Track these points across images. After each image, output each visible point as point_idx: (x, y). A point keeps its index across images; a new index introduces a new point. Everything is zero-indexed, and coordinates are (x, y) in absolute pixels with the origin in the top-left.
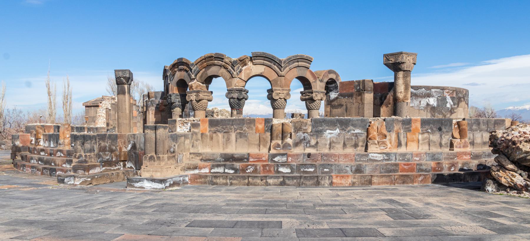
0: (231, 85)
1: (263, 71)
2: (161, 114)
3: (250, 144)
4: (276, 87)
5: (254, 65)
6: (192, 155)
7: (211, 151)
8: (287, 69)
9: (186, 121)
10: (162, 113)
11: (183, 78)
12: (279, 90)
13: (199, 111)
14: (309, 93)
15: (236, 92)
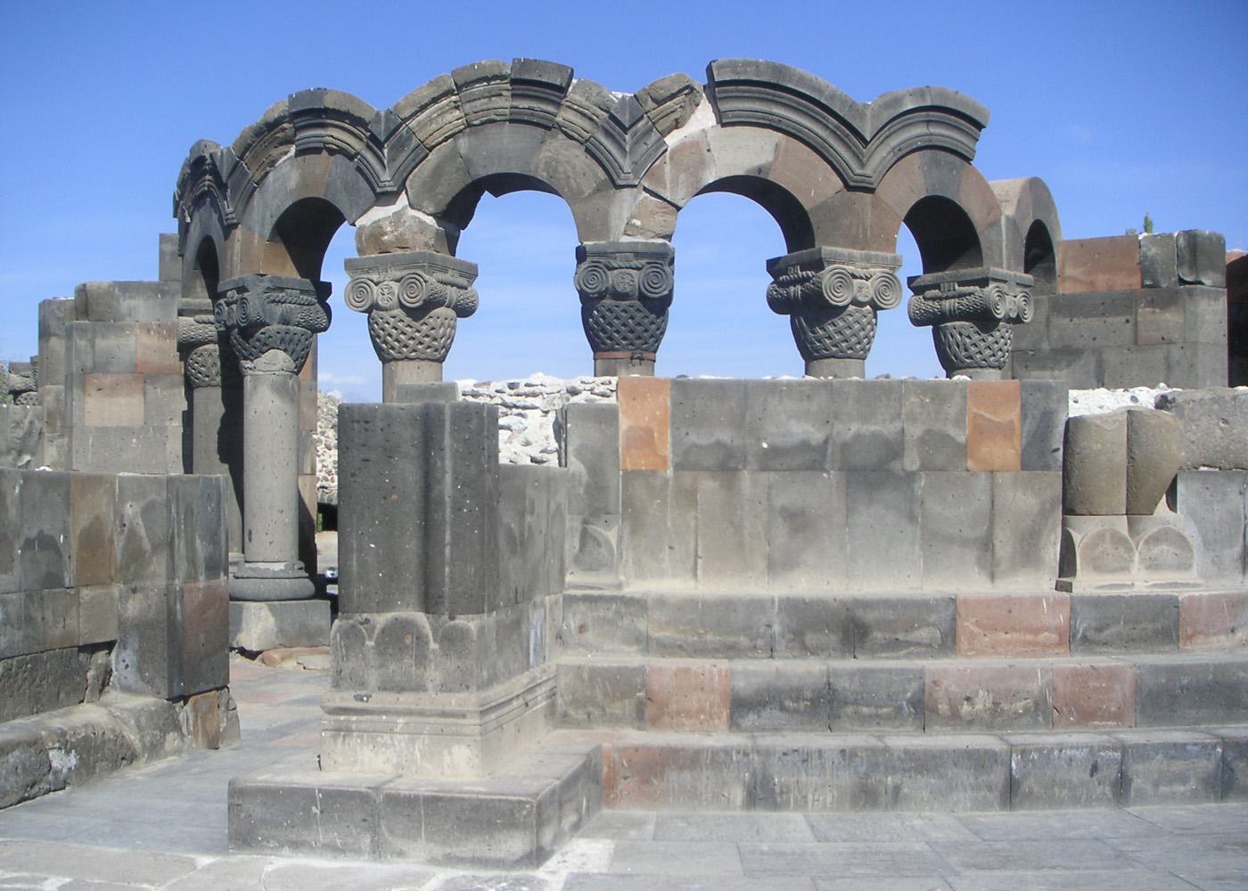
0: (603, 228)
1: (771, 159)
2: (145, 394)
3: (935, 542)
4: (836, 244)
5: (724, 125)
6: (582, 607)
7: (692, 583)
8: (883, 152)
9: (514, 400)
10: (149, 387)
11: (322, 197)
12: (851, 260)
13: (417, 363)
14: (961, 284)
15: (635, 263)
